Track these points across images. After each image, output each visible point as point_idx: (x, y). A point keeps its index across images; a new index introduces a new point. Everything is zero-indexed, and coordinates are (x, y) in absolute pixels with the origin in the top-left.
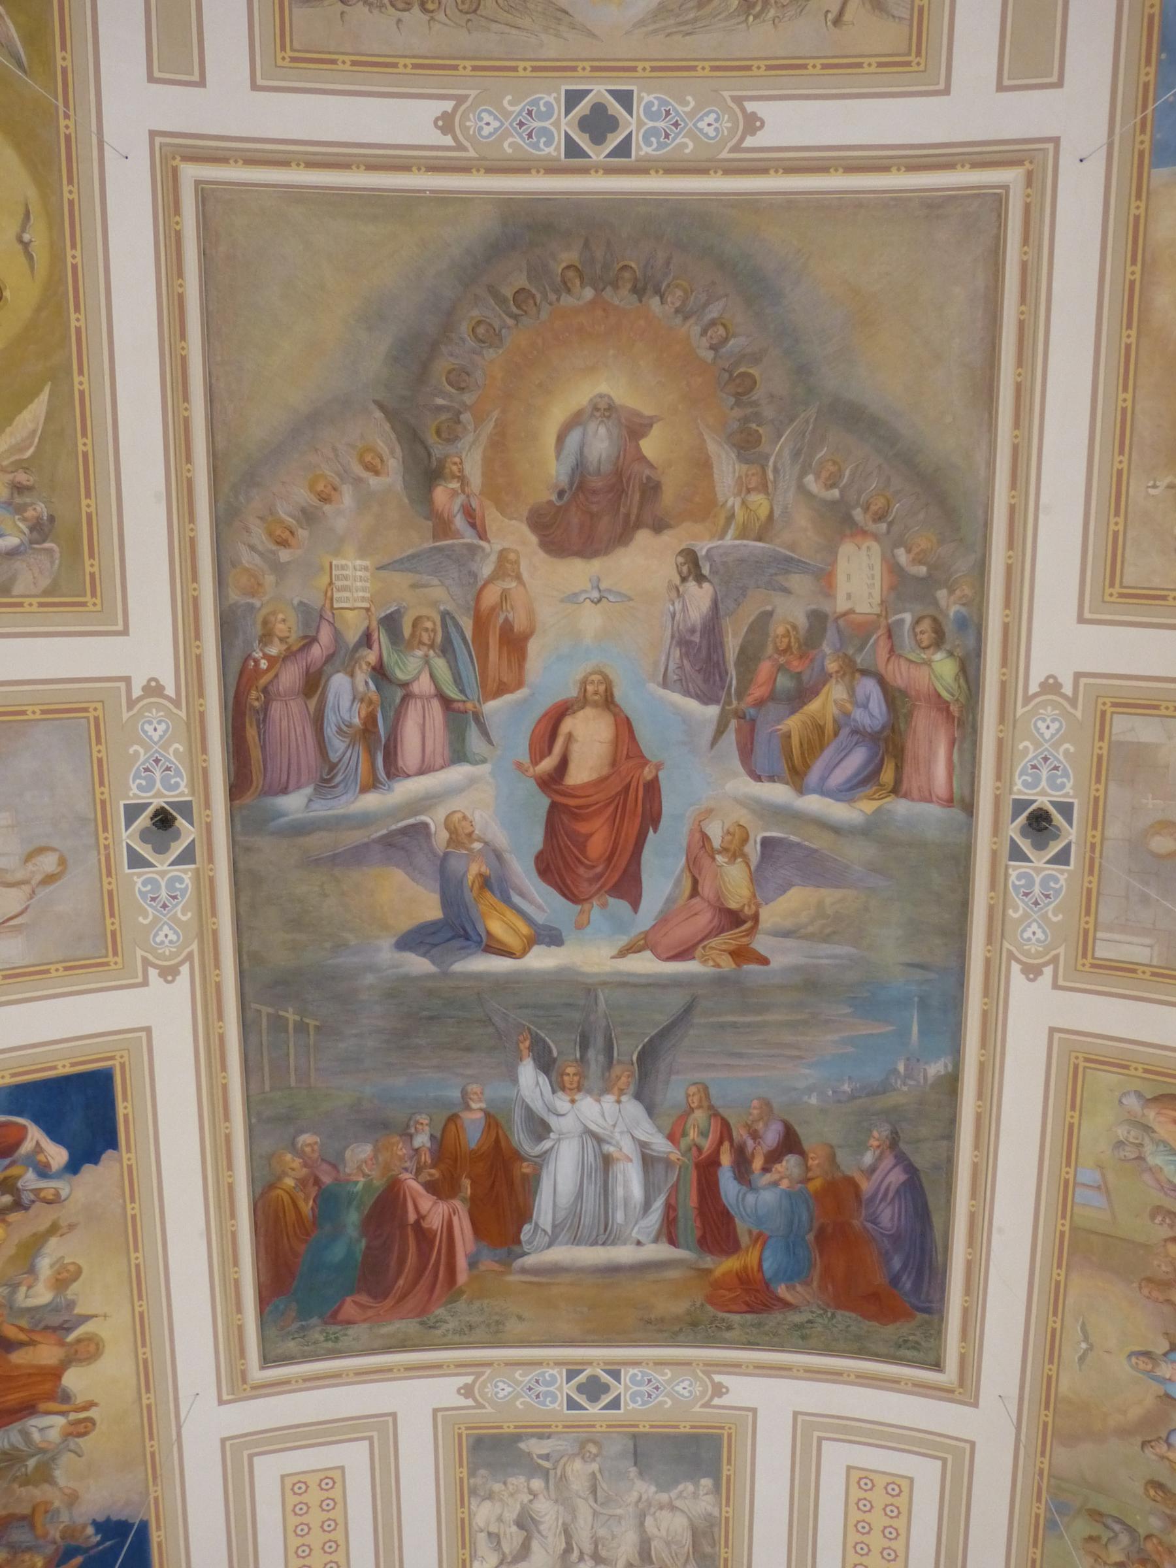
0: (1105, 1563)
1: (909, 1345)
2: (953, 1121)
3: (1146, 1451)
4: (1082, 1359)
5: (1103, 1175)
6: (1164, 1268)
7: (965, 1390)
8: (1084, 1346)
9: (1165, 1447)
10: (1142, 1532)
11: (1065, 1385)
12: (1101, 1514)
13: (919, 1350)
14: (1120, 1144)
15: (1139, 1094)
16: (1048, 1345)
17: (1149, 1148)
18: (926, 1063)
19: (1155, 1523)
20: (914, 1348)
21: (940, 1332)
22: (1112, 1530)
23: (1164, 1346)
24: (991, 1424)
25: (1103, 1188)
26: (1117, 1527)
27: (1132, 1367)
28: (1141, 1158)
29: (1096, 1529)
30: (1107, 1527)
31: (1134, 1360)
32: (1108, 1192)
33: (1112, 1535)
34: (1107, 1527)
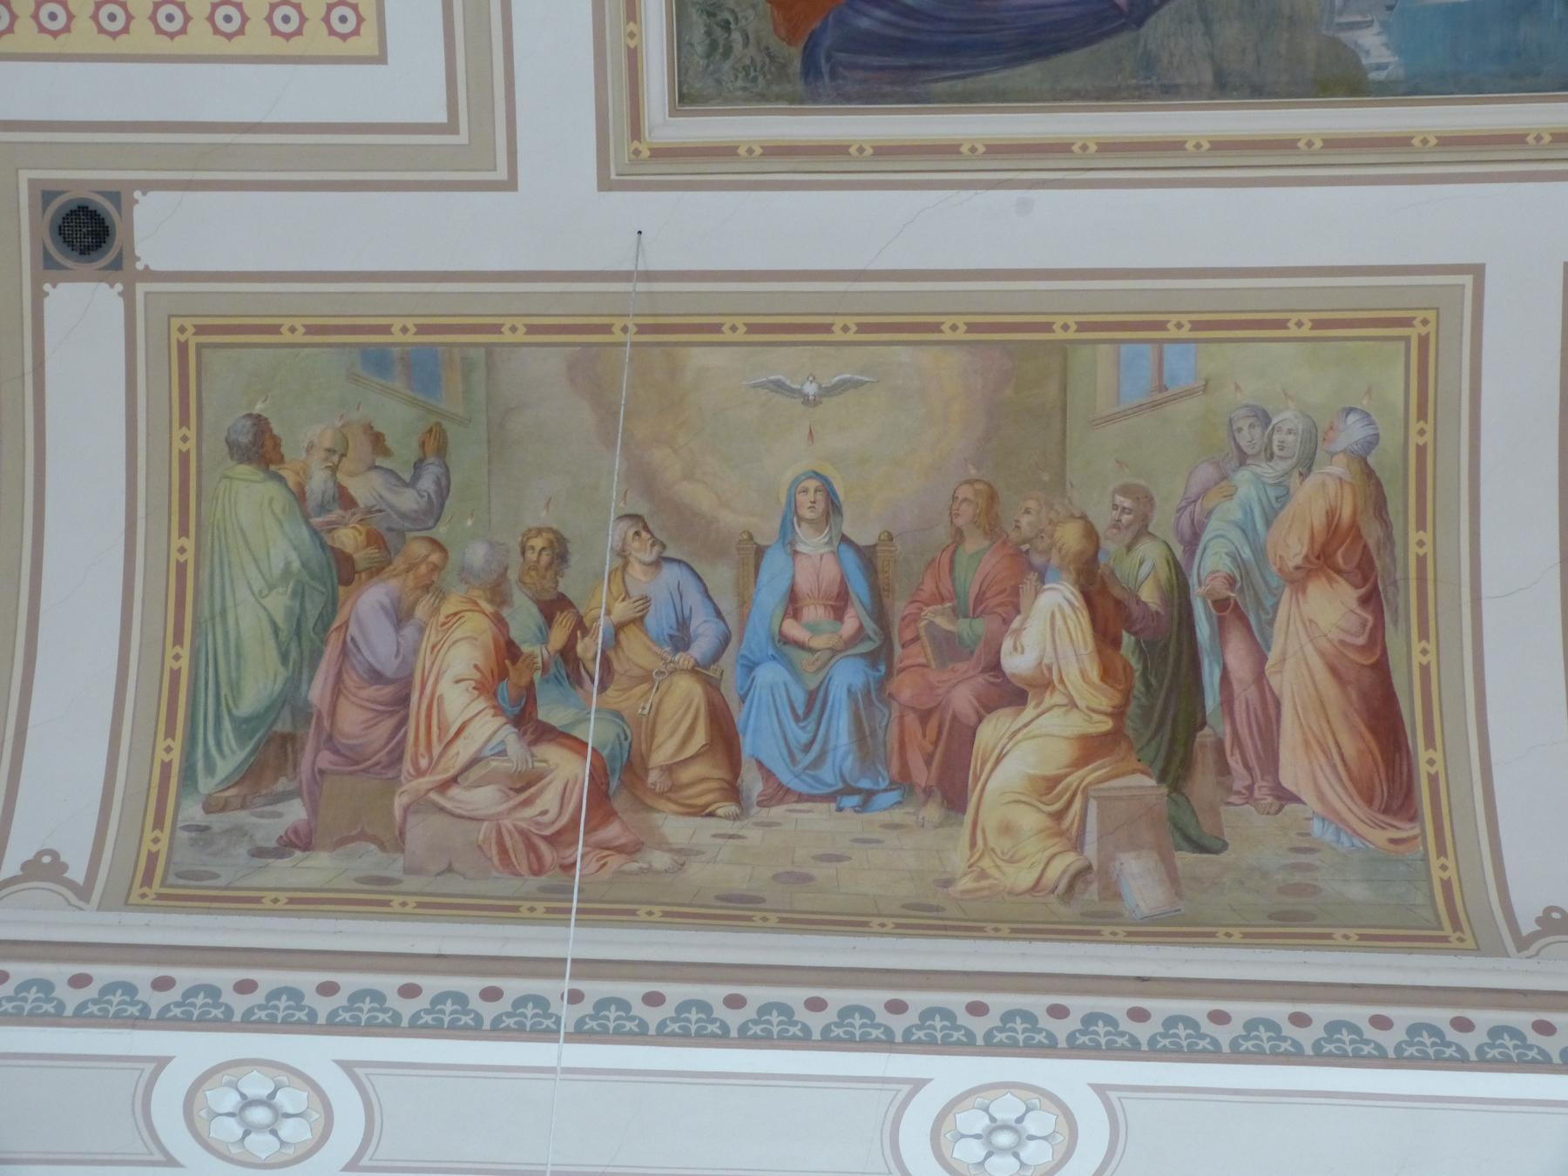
0: (334, 470)
1: (718, 32)
2: (1258, 90)
3: (624, 525)
4: (779, 386)
5: (1190, 393)
6: (1025, 521)
7: (630, 161)
8: (810, 389)
9: (649, 557)
10: (441, 532)
11: (702, 359)
12: (441, 451)
13: (709, 55)
14: (1264, 418)
15: (1372, 442)
16: (787, 319)
17: (1269, 471)
18: (1385, 26)
19: (477, 554)
20: (713, 46)
21: (762, 97)
22: (416, 477)
23: (865, 538)
24: (560, 216)
25: (1161, 396)
26: (427, 483)
27: (796, 482)
28: (1243, 459)
29: (404, 450)
30: (418, 465)
31: (812, 484)
32: (1155, 405)
33: (407, 477)
34: (418, 465)
